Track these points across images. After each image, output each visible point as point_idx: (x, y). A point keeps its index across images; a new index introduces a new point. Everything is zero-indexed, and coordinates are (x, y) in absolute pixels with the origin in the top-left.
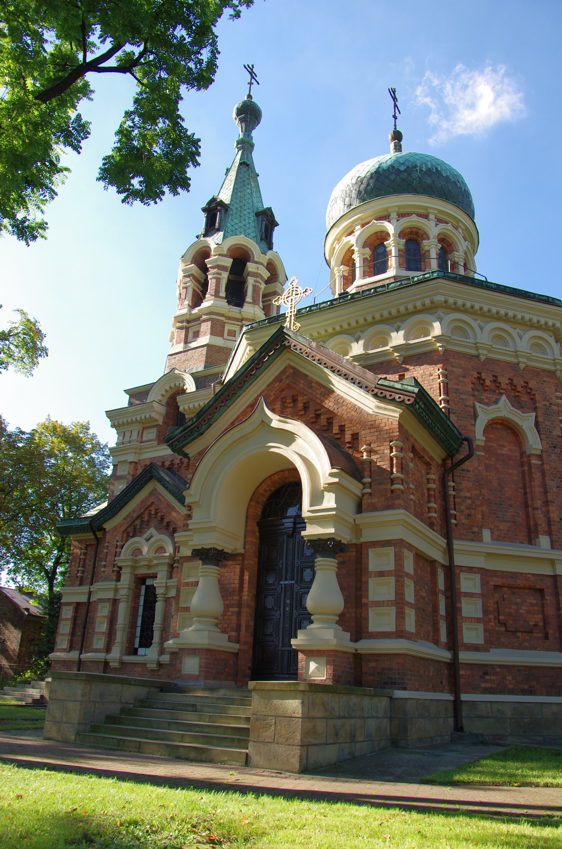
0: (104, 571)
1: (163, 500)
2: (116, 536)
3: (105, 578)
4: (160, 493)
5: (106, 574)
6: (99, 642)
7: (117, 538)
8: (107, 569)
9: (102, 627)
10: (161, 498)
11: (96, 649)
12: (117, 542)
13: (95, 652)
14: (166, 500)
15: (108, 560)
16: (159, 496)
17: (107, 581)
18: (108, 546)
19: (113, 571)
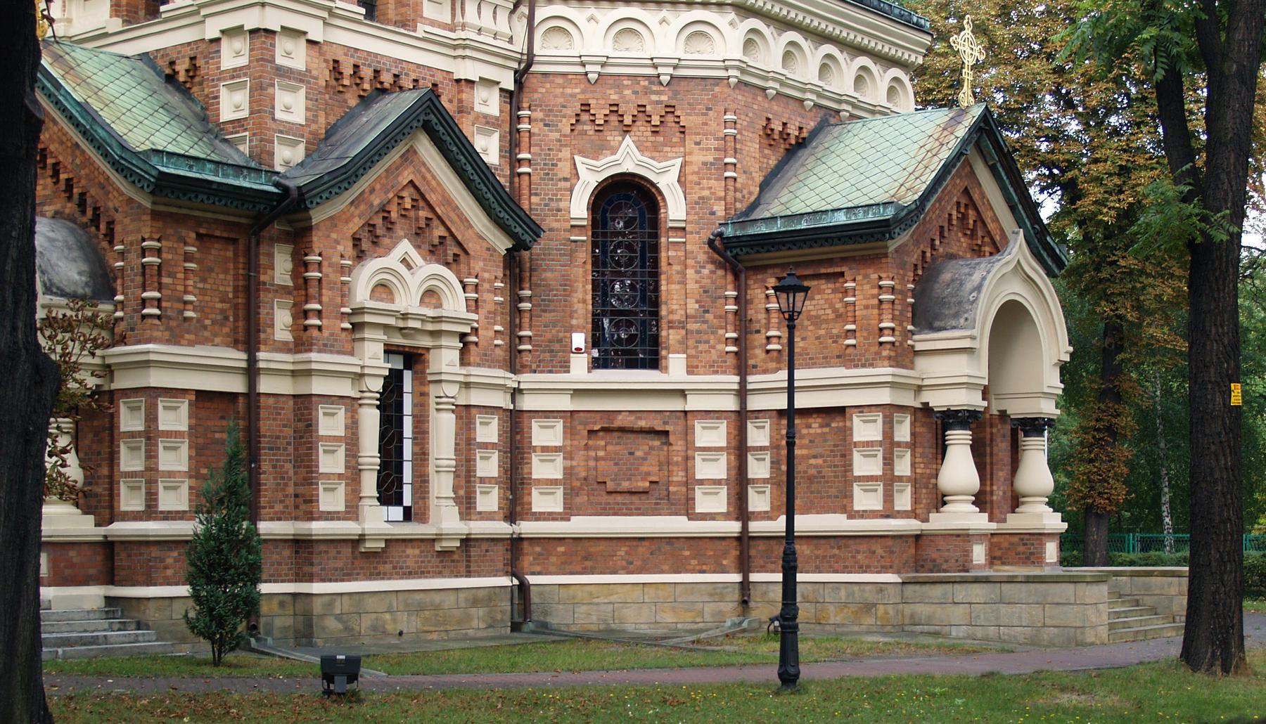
0: (320, 328)
1: (433, 183)
2: (337, 242)
3: (325, 345)
4: (424, 164)
5: (326, 333)
6: (333, 499)
7: (340, 248)
8: (325, 322)
9: (331, 463)
10: (428, 176)
11: (329, 513)
12: (342, 256)
13: (327, 519)
14: (439, 184)
15: (325, 299)
16: (423, 170)
17: (331, 352)
18: (320, 264)
19: (343, 329)
